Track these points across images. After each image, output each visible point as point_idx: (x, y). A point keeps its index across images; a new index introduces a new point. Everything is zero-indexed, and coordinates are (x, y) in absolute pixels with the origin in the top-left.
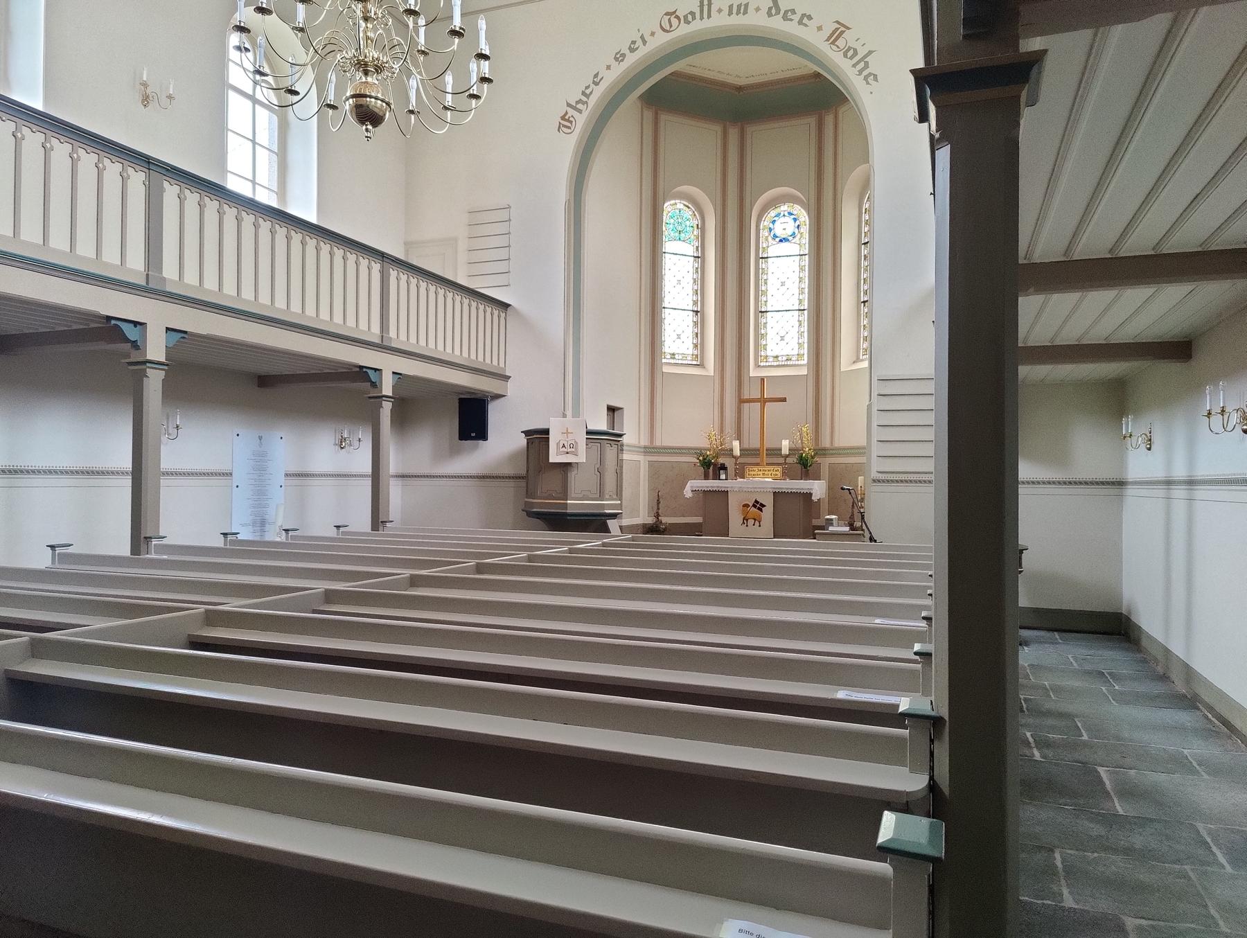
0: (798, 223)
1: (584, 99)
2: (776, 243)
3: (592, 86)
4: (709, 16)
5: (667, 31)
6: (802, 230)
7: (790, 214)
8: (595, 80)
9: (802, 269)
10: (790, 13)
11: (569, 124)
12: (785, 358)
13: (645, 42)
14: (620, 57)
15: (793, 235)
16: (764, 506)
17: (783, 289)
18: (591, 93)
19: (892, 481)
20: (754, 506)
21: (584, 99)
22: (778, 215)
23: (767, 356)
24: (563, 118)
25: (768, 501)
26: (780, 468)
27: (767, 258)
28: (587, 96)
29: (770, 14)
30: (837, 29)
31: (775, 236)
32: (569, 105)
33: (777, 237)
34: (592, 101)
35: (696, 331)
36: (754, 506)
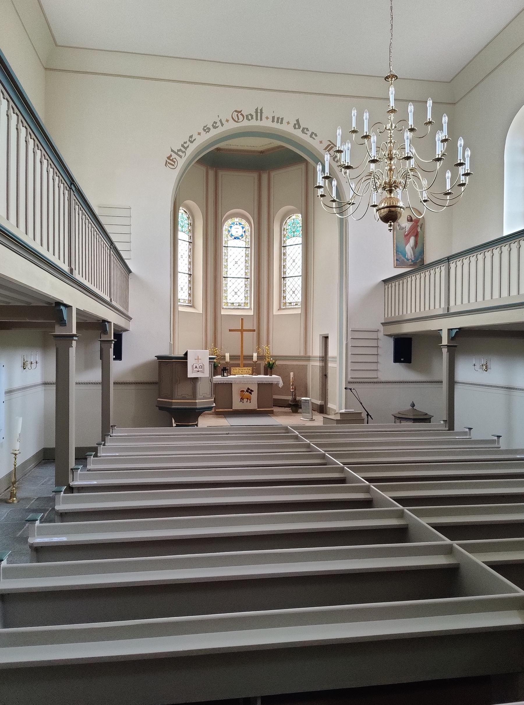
0: (244, 230)
1: (183, 150)
2: (232, 239)
3: (188, 143)
4: (261, 120)
5: (237, 122)
6: (247, 234)
7: (240, 224)
8: (191, 139)
9: (247, 256)
10: (305, 130)
11: (174, 164)
12: (237, 305)
13: (222, 125)
14: (206, 130)
15: (242, 236)
16: (252, 391)
17: (236, 265)
18: (188, 146)
19: (355, 382)
20: (247, 391)
21: (183, 150)
22: (233, 224)
23: (227, 303)
24: (169, 158)
25: (255, 388)
26: (251, 368)
27: (227, 247)
28: (186, 148)
29: (295, 128)
30: (330, 145)
31: (232, 235)
32: (172, 151)
33: (233, 236)
34: (189, 152)
36: (247, 391)
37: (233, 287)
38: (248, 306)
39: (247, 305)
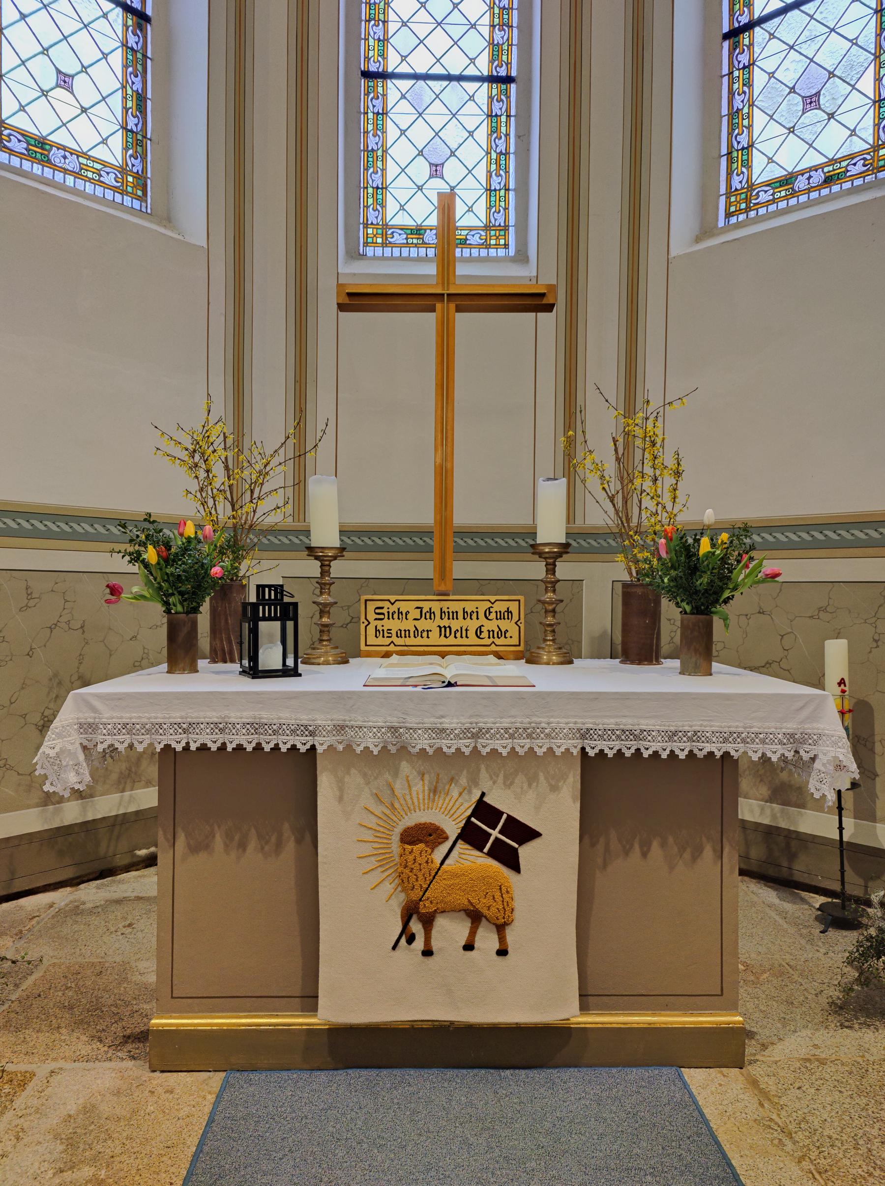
23: (386, 226)
35: (138, 86)
37: (421, 134)
38: (506, 246)
39: (502, 242)
